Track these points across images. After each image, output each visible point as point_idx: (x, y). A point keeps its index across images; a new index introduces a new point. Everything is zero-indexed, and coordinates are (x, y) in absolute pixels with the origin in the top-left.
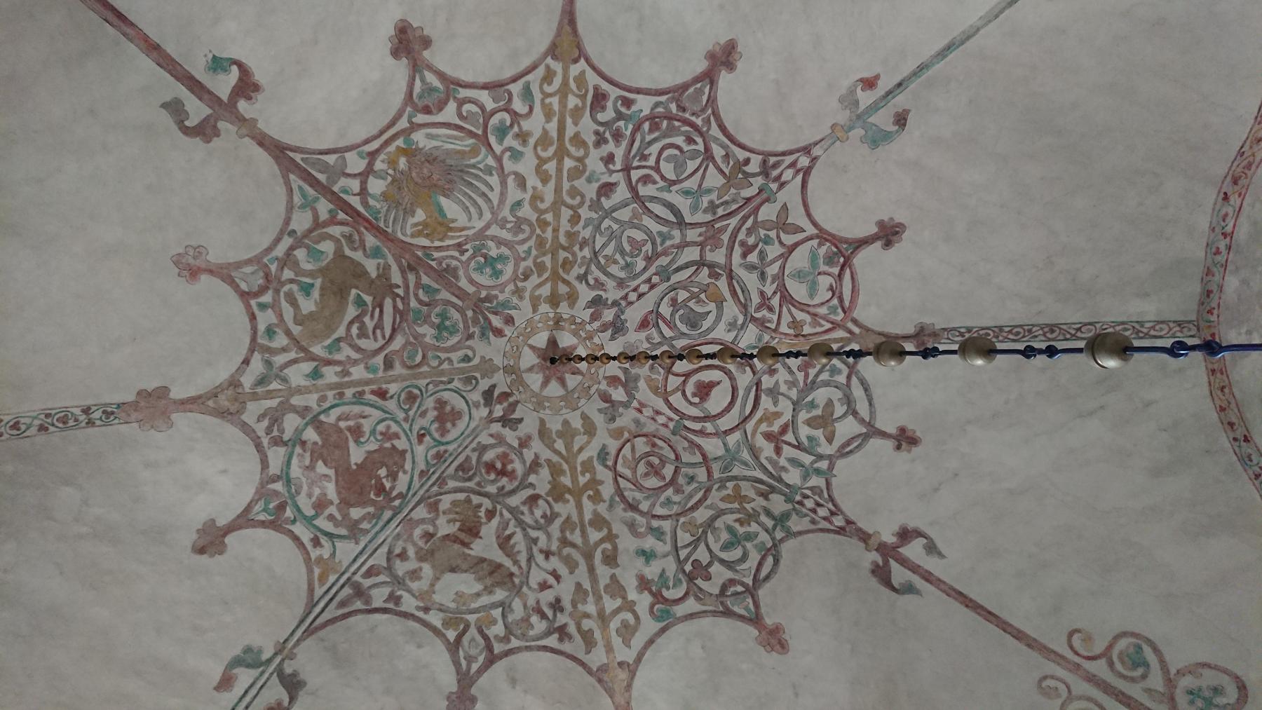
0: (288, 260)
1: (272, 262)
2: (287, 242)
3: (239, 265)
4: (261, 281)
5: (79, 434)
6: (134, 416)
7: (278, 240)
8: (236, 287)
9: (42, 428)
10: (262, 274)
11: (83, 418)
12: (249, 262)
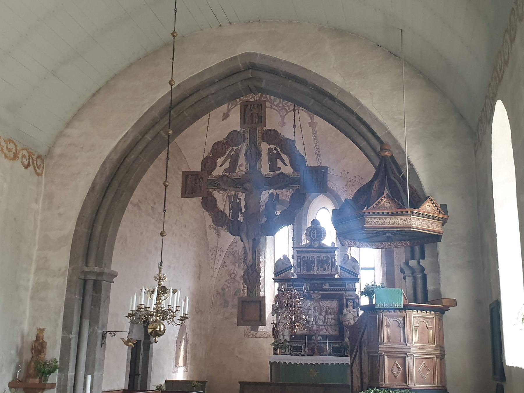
0: (277, 105)
2: (273, 107)
3: (281, 115)
4: (284, 110)
6: (314, 127)
8: (286, 115)
10: (282, 110)
11: (315, 134)
12: (280, 114)
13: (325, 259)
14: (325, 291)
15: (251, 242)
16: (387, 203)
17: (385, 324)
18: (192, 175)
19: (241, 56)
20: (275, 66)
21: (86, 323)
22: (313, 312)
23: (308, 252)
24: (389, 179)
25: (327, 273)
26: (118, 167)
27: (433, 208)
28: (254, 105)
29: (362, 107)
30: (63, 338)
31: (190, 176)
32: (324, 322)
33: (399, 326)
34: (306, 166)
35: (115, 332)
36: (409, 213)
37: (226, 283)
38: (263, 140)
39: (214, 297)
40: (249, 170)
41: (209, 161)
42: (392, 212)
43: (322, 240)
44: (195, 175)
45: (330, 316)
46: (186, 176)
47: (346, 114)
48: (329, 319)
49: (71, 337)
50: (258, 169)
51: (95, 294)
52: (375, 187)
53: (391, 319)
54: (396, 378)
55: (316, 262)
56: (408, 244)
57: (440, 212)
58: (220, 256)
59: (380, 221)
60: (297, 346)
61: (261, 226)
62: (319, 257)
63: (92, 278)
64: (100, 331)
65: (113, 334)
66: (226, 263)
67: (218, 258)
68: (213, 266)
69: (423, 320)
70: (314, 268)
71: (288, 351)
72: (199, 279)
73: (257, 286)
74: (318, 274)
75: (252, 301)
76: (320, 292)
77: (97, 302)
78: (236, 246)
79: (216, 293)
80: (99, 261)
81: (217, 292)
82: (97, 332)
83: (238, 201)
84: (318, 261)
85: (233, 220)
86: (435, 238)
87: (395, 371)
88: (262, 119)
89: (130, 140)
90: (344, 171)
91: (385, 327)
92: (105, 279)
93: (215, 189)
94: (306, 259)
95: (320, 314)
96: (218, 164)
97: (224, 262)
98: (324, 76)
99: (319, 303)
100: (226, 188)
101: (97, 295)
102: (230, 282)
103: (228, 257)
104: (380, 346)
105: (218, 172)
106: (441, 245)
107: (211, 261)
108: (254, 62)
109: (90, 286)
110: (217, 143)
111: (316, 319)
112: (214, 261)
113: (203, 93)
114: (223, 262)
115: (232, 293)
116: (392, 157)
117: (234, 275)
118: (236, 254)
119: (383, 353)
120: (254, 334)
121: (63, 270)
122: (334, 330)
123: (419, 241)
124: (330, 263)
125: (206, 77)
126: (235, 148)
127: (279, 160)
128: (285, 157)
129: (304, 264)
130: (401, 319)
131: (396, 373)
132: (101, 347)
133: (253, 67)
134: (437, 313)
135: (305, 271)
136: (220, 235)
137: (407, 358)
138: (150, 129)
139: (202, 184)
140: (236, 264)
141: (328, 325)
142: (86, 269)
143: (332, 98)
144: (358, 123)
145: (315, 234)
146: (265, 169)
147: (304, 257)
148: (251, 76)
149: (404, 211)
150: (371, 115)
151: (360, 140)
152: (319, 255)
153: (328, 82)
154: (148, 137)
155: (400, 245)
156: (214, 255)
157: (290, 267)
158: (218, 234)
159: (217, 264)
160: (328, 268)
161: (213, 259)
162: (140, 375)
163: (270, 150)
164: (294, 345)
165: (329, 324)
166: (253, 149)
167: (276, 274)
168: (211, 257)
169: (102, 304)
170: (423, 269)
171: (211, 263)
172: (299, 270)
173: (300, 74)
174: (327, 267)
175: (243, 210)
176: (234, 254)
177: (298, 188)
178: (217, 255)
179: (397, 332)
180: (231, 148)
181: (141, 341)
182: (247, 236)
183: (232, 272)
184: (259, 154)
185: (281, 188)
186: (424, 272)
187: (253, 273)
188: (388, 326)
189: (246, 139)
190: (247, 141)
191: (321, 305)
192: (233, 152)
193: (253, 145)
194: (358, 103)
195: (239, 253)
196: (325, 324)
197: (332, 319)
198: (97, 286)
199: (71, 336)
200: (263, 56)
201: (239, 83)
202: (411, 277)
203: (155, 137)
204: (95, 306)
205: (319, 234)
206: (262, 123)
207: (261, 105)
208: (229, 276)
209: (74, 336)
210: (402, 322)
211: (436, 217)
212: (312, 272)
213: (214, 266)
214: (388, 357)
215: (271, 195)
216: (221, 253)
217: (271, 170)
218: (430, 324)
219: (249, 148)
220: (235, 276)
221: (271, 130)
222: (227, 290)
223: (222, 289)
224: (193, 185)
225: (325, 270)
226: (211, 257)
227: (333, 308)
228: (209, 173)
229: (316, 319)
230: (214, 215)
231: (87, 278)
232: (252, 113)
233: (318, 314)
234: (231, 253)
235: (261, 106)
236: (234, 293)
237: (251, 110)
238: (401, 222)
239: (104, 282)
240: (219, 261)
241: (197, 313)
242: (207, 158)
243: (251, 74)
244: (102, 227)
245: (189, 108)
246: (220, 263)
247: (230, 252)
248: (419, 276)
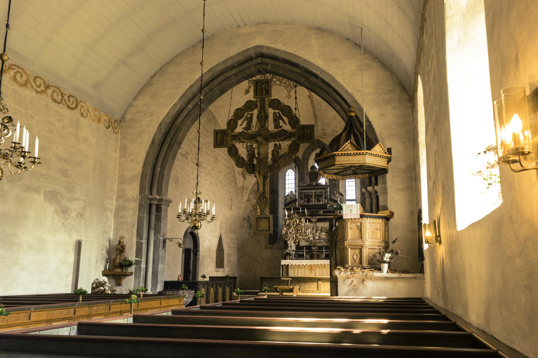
0: (285, 83)
1: (286, 86)
2: (282, 84)
3: (287, 90)
5: (315, 104)
7: (282, 86)
8: (291, 90)
9: (314, 108)
12: (287, 89)
13: (320, 194)
14: (320, 216)
15: (262, 178)
16: (350, 147)
17: (349, 227)
18: (220, 132)
19: (254, 48)
20: (277, 54)
21: (152, 233)
22: (312, 231)
23: (308, 189)
24: (354, 132)
25: (322, 203)
26: (170, 127)
27: (381, 150)
28: (263, 82)
29: (337, 82)
30: (137, 242)
31: (219, 133)
32: (319, 238)
33: (358, 229)
34: (300, 124)
35: (172, 238)
36: (365, 153)
37: (251, 212)
38: (270, 107)
40: (260, 128)
41: (232, 122)
42: (354, 153)
43: (318, 181)
44: (223, 132)
45: (323, 233)
46: (217, 133)
47: (327, 88)
48: (323, 235)
49: (142, 242)
50: (266, 127)
51: (157, 214)
52: (344, 137)
53: (353, 224)
54: (355, 262)
55: (313, 196)
56: (367, 176)
57: (385, 153)
58: (246, 194)
59: (346, 159)
60: (301, 254)
61: (269, 166)
62: (316, 192)
63: (155, 203)
64: (162, 238)
65: (171, 240)
67: (245, 195)
68: (241, 200)
69: (375, 225)
70: (312, 201)
71: (294, 257)
72: (231, 209)
73: (266, 208)
74: (315, 204)
75: (263, 218)
76: (317, 217)
77: (158, 219)
80: (159, 192)
82: (159, 239)
83: (253, 150)
84: (315, 195)
85: (249, 163)
86: (384, 171)
87: (355, 257)
88: (268, 92)
89: (177, 108)
90: (334, 130)
91: (349, 230)
92: (163, 204)
93: (236, 142)
94: (307, 194)
95: (316, 232)
96: (239, 124)
98: (310, 61)
99: (316, 225)
100: (244, 141)
101: (159, 214)
102: (253, 211)
103: (252, 194)
104: (345, 242)
105: (239, 129)
106: (389, 176)
107: (239, 197)
108: (262, 51)
109: (154, 209)
110: (238, 109)
111: (314, 235)
113: (228, 74)
114: (248, 198)
116: (356, 116)
119: (348, 246)
120: (271, 247)
121: (135, 197)
122: (326, 242)
123: (374, 174)
124: (324, 197)
125: (229, 63)
126: (250, 113)
127: (281, 121)
128: (285, 118)
129: (305, 198)
130: (359, 224)
131: (355, 259)
132: (163, 249)
133: (262, 55)
134: (384, 220)
135: (306, 203)
137: (363, 249)
138: (191, 101)
139: (228, 139)
141: (323, 239)
142: (150, 197)
143: (316, 76)
144: (334, 94)
145: (314, 176)
146: (271, 127)
147: (305, 193)
148: (260, 62)
149: (361, 152)
150: (343, 88)
151: (336, 105)
152: (316, 191)
153: (314, 65)
154: (190, 106)
155: (362, 177)
156: (241, 193)
157: (295, 200)
159: (244, 199)
160: (322, 200)
161: (241, 195)
162: (191, 272)
163: (275, 114)
164: (298, 253)
165: (323, 238)
166: (263, 113)
167: (286, 205)
169: (162, 221)
170: (376, 192)
171: (240, 198)
172: (302, 202)
173: (294, 60)
174: (321, 199)
175: (256, 156)
177: (294, 140)
178: (244, 193)
179: (357, 232)
180: (247, 113)
181: (191, 249)
182: (259, 174)
184: (267, 117)
185: (282, 140)
186: (377, 194)
187: (263, 199)
188: (351, 229)
189: (258, 106)
190: (258, 108)
191: (318, 225)
192: (249, 116)
193: (262, 110)
194: (334, 79)
196: (320, 239)
197: (325, 235)
198: (159, 209)
199: (142, 241)
200: (268, 48)
201: (252, 67)
202: (369, 198)
203: (194, 106)
204: (157, 221)
205: (316, 176)
206: (268, 94)
207: (268, 82)
208: (252, 207)
209: (144, 241)
210: (360, 226)
211: (383, 156)
212: (311, 203)
214: (351, 249)
215: (275, 145)
216: (247, 191)
217: (276, 127)
218: (379, 227)
219: (260, 112)
221: (275, 99)
222: (251, 217)
223: (248, 216)
224: (222, 139)
225: (320, 201)
226: (239, 193)
227: (326, 228)
228: (233, 131)
229: (314, 235)
230: (237, 160)
231: (152, 203)
232: (262, 88)
233: (315, 232)
235: (268, 83)
237: (262, 86)
238: (360, 159)
239: (163, 205)
241: (231, 233)
242: (231, 120)
243: (261, 60)
244: (161, 168)
245: (217, 85)
246: (246, 198)
247: (253, 190)
248: (374, 197)
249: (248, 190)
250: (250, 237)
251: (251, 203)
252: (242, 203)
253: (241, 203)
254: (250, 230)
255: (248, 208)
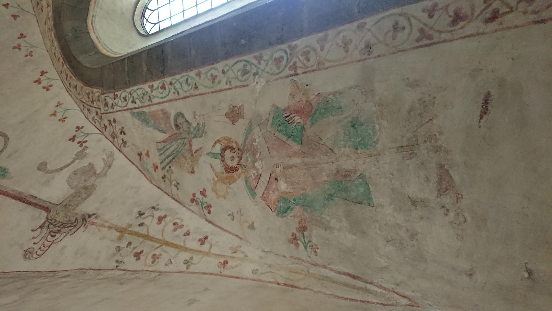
37: (260, 190)
39: (319, 261)
58: (168, 219)
66: (194, 195)
68: (185, 256)
78: (147, 155)
79: (301, 246)
81: (297, 245)
97: (193, 201)
112: (164, 247)
114: (194, 207)
115: (295, 154)
117: (228, 153)
118: (169, 151)
136: (90, 216)
140: (194, 148)
156: (147, 247)
158: (79, 225)
161: (157, 252)
168: (146, 259)
176: (167, 161)
178: (154, 230)
183: (218, 165)
195: (164, 141)
213: (186, 249)
216: (157, 214)
220: (232, 149)
223: (283, 212)
226: (138, 265)
234: (166, 174)
236: (296, 147)
240: (182, 226)
249: (153, 208)
250: (447, 200)
251: (214, 190)
252: (206, 247)
253: (196, 258)
254: (377, 199)
255: (240, 212)
